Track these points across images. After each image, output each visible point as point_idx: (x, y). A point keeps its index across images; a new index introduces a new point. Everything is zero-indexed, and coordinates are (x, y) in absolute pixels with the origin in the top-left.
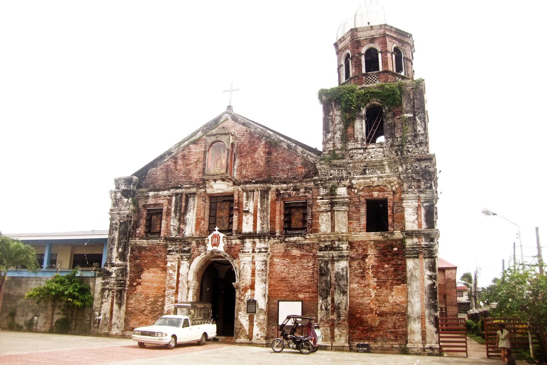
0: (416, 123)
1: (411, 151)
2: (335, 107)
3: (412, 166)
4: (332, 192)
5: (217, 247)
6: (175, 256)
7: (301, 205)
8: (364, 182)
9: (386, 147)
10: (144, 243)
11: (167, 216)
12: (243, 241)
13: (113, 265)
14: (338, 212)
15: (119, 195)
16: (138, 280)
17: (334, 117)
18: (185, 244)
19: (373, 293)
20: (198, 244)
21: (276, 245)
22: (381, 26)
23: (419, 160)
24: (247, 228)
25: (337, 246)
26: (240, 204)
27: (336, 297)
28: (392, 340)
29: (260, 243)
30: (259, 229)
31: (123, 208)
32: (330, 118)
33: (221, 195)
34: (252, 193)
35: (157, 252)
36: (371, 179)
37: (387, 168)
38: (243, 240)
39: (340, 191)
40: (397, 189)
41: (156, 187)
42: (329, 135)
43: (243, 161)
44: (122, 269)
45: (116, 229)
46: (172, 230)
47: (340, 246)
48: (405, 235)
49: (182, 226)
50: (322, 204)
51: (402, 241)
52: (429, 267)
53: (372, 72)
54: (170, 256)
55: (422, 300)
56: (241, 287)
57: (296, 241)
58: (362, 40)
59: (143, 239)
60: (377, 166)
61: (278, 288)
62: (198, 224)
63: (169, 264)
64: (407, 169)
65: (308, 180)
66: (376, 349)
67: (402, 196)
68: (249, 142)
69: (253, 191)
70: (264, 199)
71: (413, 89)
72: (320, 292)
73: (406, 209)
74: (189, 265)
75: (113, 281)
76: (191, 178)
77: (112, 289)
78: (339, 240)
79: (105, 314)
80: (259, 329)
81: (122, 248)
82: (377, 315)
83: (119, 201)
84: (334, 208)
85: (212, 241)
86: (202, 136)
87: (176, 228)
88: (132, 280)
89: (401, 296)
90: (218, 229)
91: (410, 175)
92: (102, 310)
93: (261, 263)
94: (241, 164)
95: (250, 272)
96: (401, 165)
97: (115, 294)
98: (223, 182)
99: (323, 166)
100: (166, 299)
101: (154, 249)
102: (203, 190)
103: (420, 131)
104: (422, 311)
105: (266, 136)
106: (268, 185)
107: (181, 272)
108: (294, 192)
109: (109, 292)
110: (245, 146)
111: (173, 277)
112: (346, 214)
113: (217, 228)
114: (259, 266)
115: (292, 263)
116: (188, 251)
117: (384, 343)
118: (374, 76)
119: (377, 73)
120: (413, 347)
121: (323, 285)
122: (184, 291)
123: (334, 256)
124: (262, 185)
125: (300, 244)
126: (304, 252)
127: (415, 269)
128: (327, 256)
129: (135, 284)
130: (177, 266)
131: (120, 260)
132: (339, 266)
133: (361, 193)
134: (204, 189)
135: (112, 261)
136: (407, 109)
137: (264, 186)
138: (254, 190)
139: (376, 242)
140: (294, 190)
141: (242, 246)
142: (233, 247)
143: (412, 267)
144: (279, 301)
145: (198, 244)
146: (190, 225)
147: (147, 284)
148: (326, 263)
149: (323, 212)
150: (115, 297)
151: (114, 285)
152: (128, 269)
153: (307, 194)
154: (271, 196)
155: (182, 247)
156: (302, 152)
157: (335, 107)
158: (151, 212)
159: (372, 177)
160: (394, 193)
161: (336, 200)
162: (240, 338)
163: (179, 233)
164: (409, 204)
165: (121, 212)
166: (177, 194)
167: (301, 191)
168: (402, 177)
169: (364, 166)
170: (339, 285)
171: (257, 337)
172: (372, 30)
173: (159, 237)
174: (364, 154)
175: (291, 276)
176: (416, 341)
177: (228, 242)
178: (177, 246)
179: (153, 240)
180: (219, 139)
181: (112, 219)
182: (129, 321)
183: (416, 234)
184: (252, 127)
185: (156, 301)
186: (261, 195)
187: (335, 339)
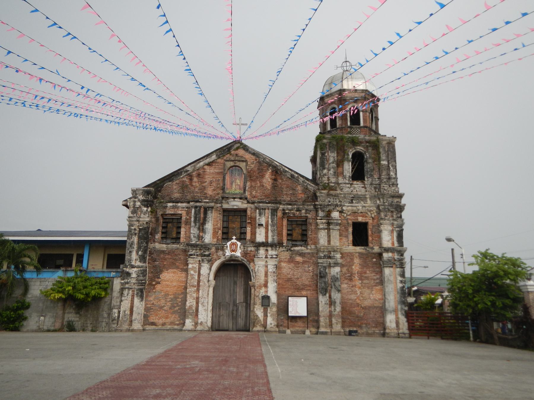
0: (389, 169)
1: (386, 189)
2: (329, 150)
3: (387, 200)
4: (328, 215)
5: (235, 252)
6: (197, 259)
7: (301, 223)
8: (352, 209)
9: (367, 185)
10: (164, 247)
11: (185, 225)
12: (258, 248)
13: (133, 267)
14: (333, 230)
15: (138, 204)
16: (156, 279)
17: (328, 157)
19: (359, 292)
20: (217, 249)
21: (283, 252)
22: (363, 90)
23: (393, 197)
24: (260, 237)
25: (333, 255)
26: (254, 219)
27: (332, 294)
28: (374, 327)
30: (270, 240)
31: (142, 215)
32: (326, 158)
33: (233, 210)
34: (264, 211)
35: (176, 255)
36: (358, 207)
37: (368, 200)
39: (335, 214)
40: (375, 216)
41: (172, 199)
42: (325, 171)
43: (253, 184)
44: (144, 270)
45: (136, 234)
46: (192, 237)
47: (335, 256)
48: (383, 250)
49: (201, 234)
50: (322, 223)
51: (380, 255)
52: (400, 274)
53: (356, 126)
54: (192, 259)
55: (395, 298)
56: (256, 285)
58: (348, 99)
59: (163, 244)
60: (361, 198)
61: (285, 286)
62: (215, 233)
63: (190, 266)
64: (384, 202)
65: (309, 204)
66: (363, 334)
67: (381, 222)
68: (258, 169)
69: (265, 209)
70: (274, 216)
71: (387, 143)
72: (321, 290)
73: (383, 231)
74: (209, 267)
75: (134, 281)
76: (206, 194)
77: (131, 288)
78: (334, 251)
79: (125, 312)
80: (272, 319)
81: (142, 251)
82: (362, 309)
83: (137, 209)
84: (330, 227)
85: (231, 247)
86: (216, 159)
87: (196, 235)
88: (151, 280)
89: (379, 295)
91: (386, 207)
92: (121, 308)
93: (273, 266)
94: (251, 186)
95: (263, 274)
96: (379, 199)
97: (135, 293)
98: (240, 200)
99: (322, 194)
100: (188, 296)
101: (174, 252)
102: (219, 205)
103: (392, 175)
104: (396, 306)
105: (272, 166)
106: (278, 205)
107: (202, 272)
108: (298, 213)
109: (129, 291)
110: (254, 172)
112: (338, 233)
113: (234, 237)
114: (271, 268)
115: (296, 267)
116: (208, 256)
117: (368, 329)
118: (356, 129)
119: (359, 127)
120: (391, 332)
121: (323, 285)
123: (331, 263)
124: (273, 205)
125: (302, 253)
126: (305, 259)
127: (390, 276)
128: (326, 263)
129: (154, 283)
130: (197, 267)
131: (140, 262)
132: (335, 271)
133: (348, 217)
135: (131, 263)
136: (383, 158)
137: (275, 205)
139: (361, 254)
140: (297, 211)
143: (388, 274)
144: (288, 297)
147: (167, 283)
148: (325, 268)
149: (321, 229)
150: (135, 295)
151: (134, 284)
152: (147, 270)
153: (307, 215)
154: (280, 214)
155: (202, 252)
156: (303, 182)
157: (329, 150)
158: (167, 221)
159: (358, 206)
160: (373, 218)
161: (332, 221)
162: (256, 327)
163: (199, 240)
164: (386, 228)
165: (140, 219)
166: (196, 207)
167: (303, 212)
168: (381, 208)
169: (351, 197)
170: (334, 285)
171: (271, 326)
172: (356, 92)
173: (178, 243)
174: (351, 188)
175: (296, 277)
176: (392, 328)
177: (244, 249)
179: (174, 245)
180: (236, 164)
181: (130, 225)
182: (149, 317)
183: (391, 250)
184: (262, 157)
185: (176, 298)
186: (272, 213)
187: (333, 326)
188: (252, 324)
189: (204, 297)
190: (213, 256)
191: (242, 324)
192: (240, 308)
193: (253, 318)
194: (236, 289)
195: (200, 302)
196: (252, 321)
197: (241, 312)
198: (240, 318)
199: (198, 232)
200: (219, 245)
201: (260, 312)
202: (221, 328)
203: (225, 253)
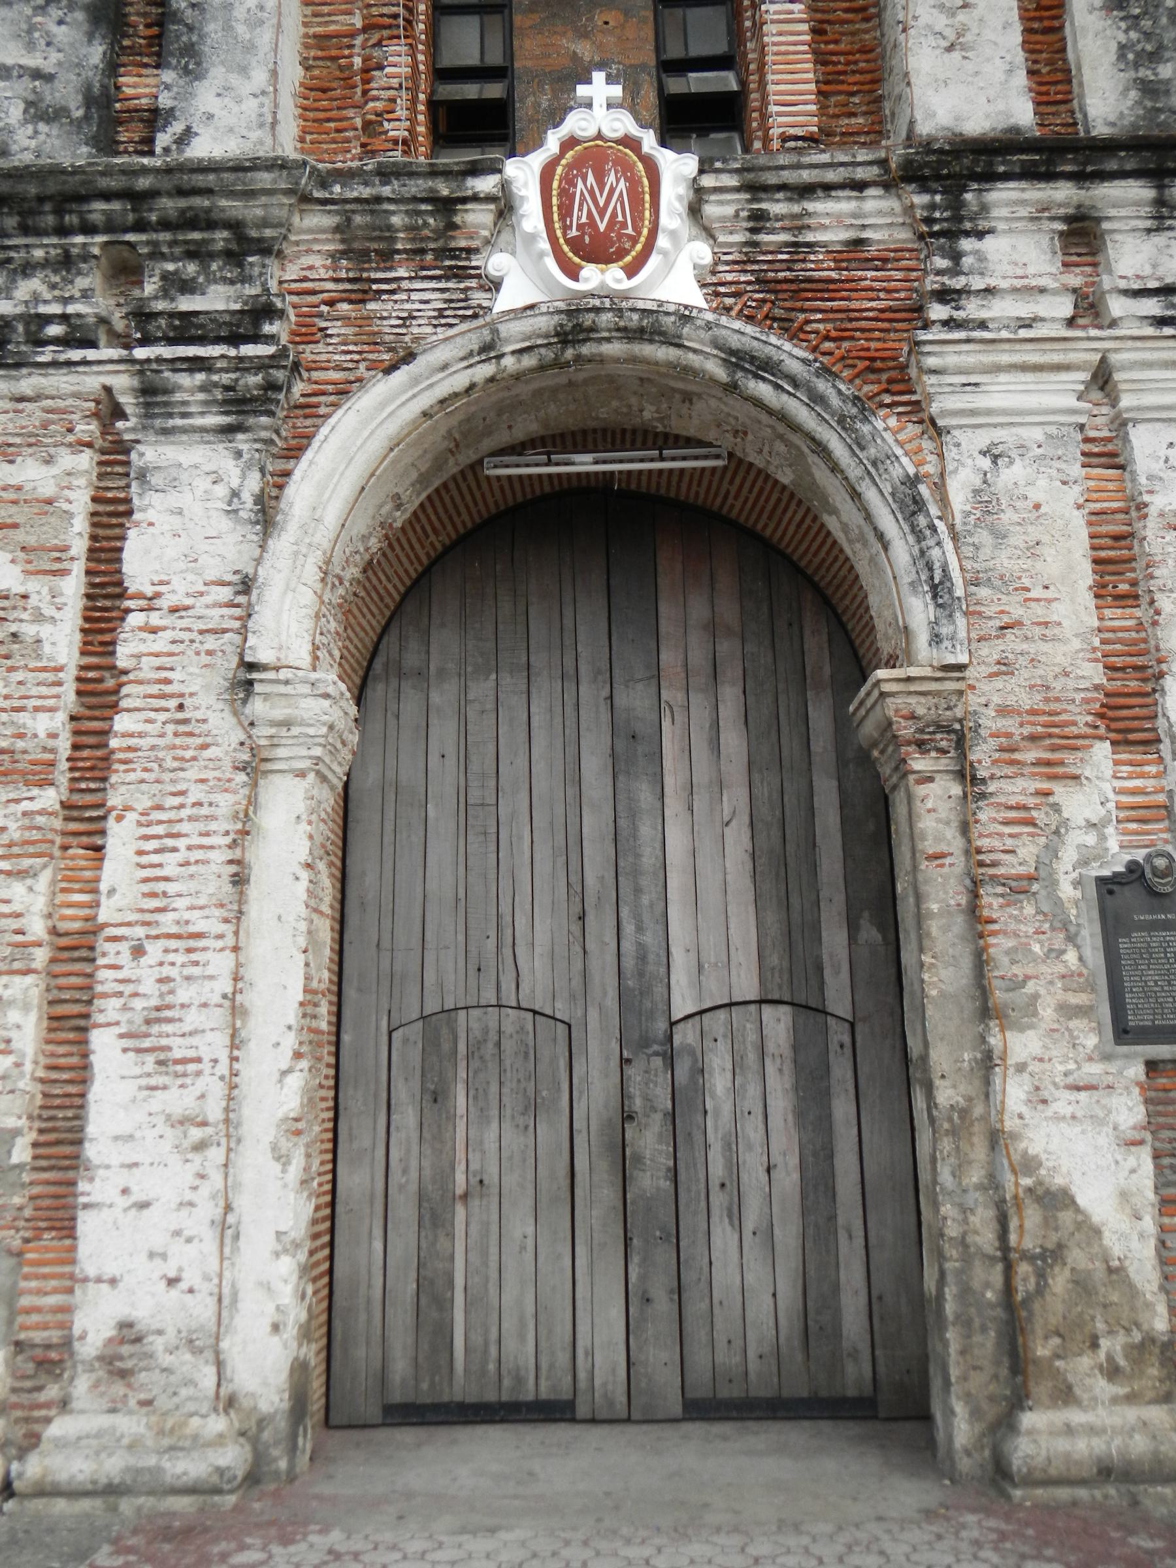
5: (631, 271)
12: (956, 205)
18: (194, 253)
29: (1160, 239)
38: (954, 186)
56: (989, 722)
74: (254, 483)
90: (617, 91)
111: (29, 630)
122: (196, 793)
130: (80, 502)
141: (941, 263)
142: (826, 288)
145: (361, 256)
146: (244, 70)
162: (1065, 1395)
163: (106, 144)
177: (759, 220)
178: (82, 282)
188: (987, 1342)
189: (167, 922)
190: (309, 353)
191: (761, 1308)
192: (719, 1082)
193: (986, 1239)
194: (646, 830)
195: (109, 1009)
196: (965, 1292)
197: (732, 1144)
198: (736, 1215)
199: (96, 53)
200: (385, 174)
201: (1105, 1139)
202: (461, 1388)
203: (479, 298)
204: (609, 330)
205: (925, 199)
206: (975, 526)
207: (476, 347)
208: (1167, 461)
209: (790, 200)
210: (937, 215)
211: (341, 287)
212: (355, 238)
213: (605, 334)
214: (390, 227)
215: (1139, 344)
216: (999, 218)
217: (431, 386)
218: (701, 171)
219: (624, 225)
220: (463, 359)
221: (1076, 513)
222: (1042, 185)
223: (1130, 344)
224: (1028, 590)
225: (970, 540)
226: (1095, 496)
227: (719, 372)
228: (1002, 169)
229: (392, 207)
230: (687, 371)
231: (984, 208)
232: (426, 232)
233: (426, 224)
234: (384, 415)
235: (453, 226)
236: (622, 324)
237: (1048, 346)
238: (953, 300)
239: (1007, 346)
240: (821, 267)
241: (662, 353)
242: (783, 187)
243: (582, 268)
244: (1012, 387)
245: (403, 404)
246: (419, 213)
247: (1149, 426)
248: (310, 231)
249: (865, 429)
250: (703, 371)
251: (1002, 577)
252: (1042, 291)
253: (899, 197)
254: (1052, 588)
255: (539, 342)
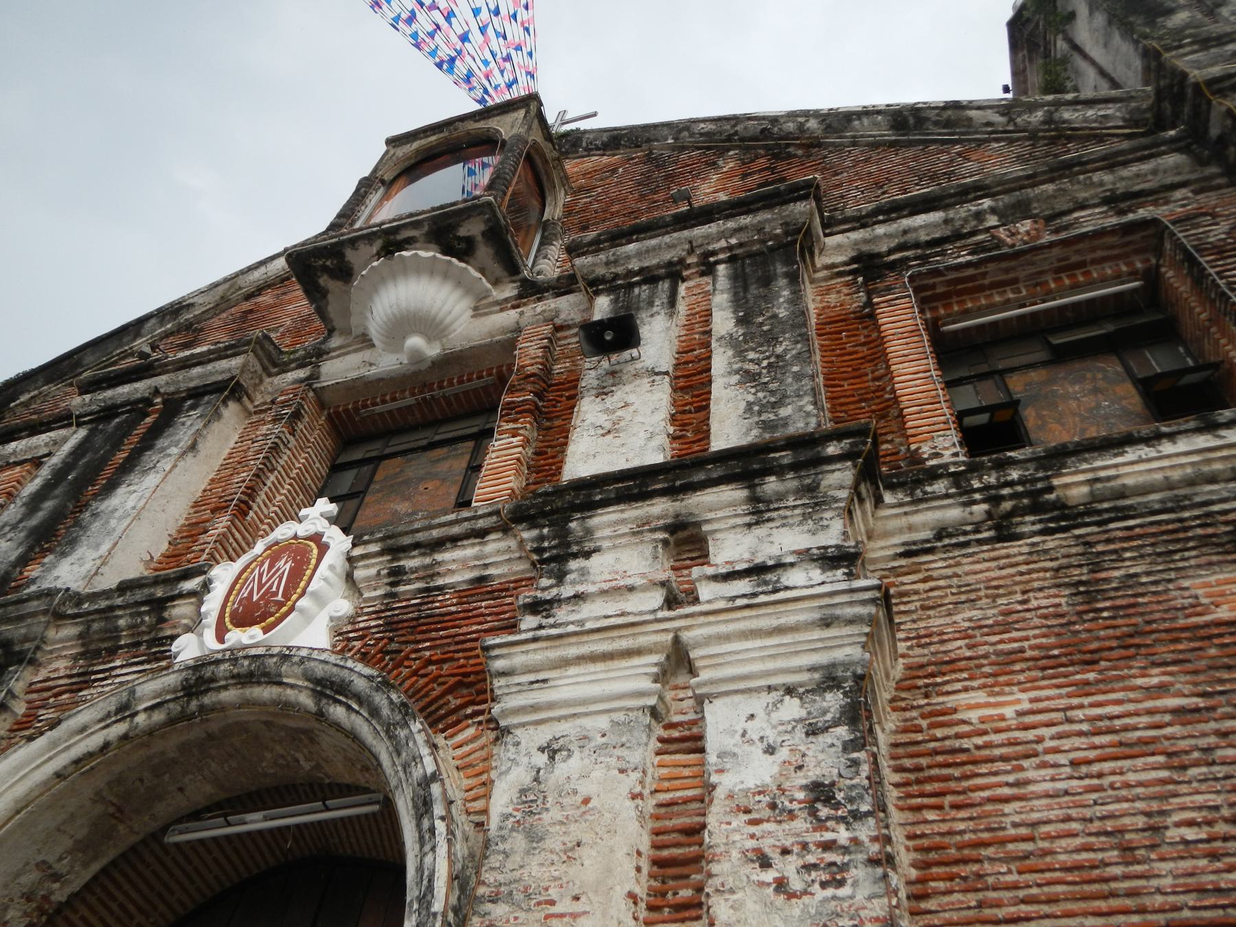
12: (563, 535)
21: (936, 563)
57: (1191, 482)
93: (792, 709)
105: (742, 139)
134: (301, 366)
138: (681, 261)
177: (397, 575)
184: (665, 131)
204: (226, 679)
205: (534, 533)
206: (512, 830)
207: (113, 708)
208: (744, 734)
209: (423, 555)
210: (546, 544)
211: (74, 680)
212: (91, 642)
213: (223, 683)
214: (117, 629)
215: (711, 618)
216: (603, 538)
217: (68, 748)
218: (354, 545)
219: (276, 594)
220: (101, 721)
221: (629, 804)
222: (640, 504)
223: (702, 619)
224: (552, 903)
225: (501, 847)
226: (666, 784)
227: (306, 700)
228: (598, 497)
229: (120, 613)
230: (287, 707)
231: (589, 532)
232: (144, 628)
233: (143, 622)
234: (17, 777)
235: (162, 620)
236: (235, 671)
237: (615, 633)
238: (546, 610)
239: (573, 640)
240: (448, 604)
241: (266, 693)
242: (417, 545)
243: (229, 631)
244: (580, 679)
245: (38, 767)
246: (140, 614)
247: (727, 700)
248: (61, 641)
249: (402, 733)
250: (298, 704)
251: (526, 888)
252: (631, 589)
253: (515, 536)
254: (583, 899)
255: (168, 697)
